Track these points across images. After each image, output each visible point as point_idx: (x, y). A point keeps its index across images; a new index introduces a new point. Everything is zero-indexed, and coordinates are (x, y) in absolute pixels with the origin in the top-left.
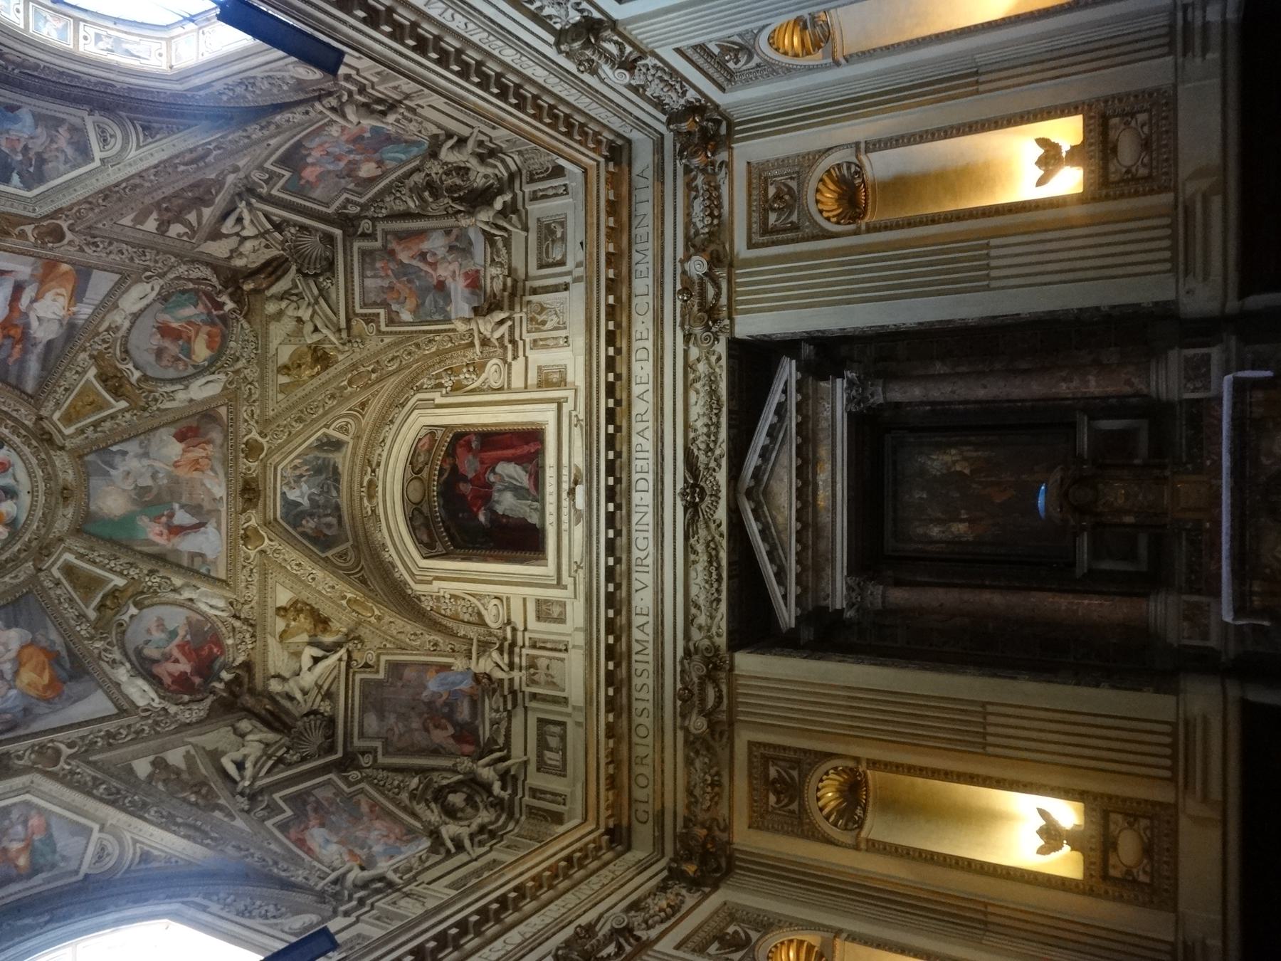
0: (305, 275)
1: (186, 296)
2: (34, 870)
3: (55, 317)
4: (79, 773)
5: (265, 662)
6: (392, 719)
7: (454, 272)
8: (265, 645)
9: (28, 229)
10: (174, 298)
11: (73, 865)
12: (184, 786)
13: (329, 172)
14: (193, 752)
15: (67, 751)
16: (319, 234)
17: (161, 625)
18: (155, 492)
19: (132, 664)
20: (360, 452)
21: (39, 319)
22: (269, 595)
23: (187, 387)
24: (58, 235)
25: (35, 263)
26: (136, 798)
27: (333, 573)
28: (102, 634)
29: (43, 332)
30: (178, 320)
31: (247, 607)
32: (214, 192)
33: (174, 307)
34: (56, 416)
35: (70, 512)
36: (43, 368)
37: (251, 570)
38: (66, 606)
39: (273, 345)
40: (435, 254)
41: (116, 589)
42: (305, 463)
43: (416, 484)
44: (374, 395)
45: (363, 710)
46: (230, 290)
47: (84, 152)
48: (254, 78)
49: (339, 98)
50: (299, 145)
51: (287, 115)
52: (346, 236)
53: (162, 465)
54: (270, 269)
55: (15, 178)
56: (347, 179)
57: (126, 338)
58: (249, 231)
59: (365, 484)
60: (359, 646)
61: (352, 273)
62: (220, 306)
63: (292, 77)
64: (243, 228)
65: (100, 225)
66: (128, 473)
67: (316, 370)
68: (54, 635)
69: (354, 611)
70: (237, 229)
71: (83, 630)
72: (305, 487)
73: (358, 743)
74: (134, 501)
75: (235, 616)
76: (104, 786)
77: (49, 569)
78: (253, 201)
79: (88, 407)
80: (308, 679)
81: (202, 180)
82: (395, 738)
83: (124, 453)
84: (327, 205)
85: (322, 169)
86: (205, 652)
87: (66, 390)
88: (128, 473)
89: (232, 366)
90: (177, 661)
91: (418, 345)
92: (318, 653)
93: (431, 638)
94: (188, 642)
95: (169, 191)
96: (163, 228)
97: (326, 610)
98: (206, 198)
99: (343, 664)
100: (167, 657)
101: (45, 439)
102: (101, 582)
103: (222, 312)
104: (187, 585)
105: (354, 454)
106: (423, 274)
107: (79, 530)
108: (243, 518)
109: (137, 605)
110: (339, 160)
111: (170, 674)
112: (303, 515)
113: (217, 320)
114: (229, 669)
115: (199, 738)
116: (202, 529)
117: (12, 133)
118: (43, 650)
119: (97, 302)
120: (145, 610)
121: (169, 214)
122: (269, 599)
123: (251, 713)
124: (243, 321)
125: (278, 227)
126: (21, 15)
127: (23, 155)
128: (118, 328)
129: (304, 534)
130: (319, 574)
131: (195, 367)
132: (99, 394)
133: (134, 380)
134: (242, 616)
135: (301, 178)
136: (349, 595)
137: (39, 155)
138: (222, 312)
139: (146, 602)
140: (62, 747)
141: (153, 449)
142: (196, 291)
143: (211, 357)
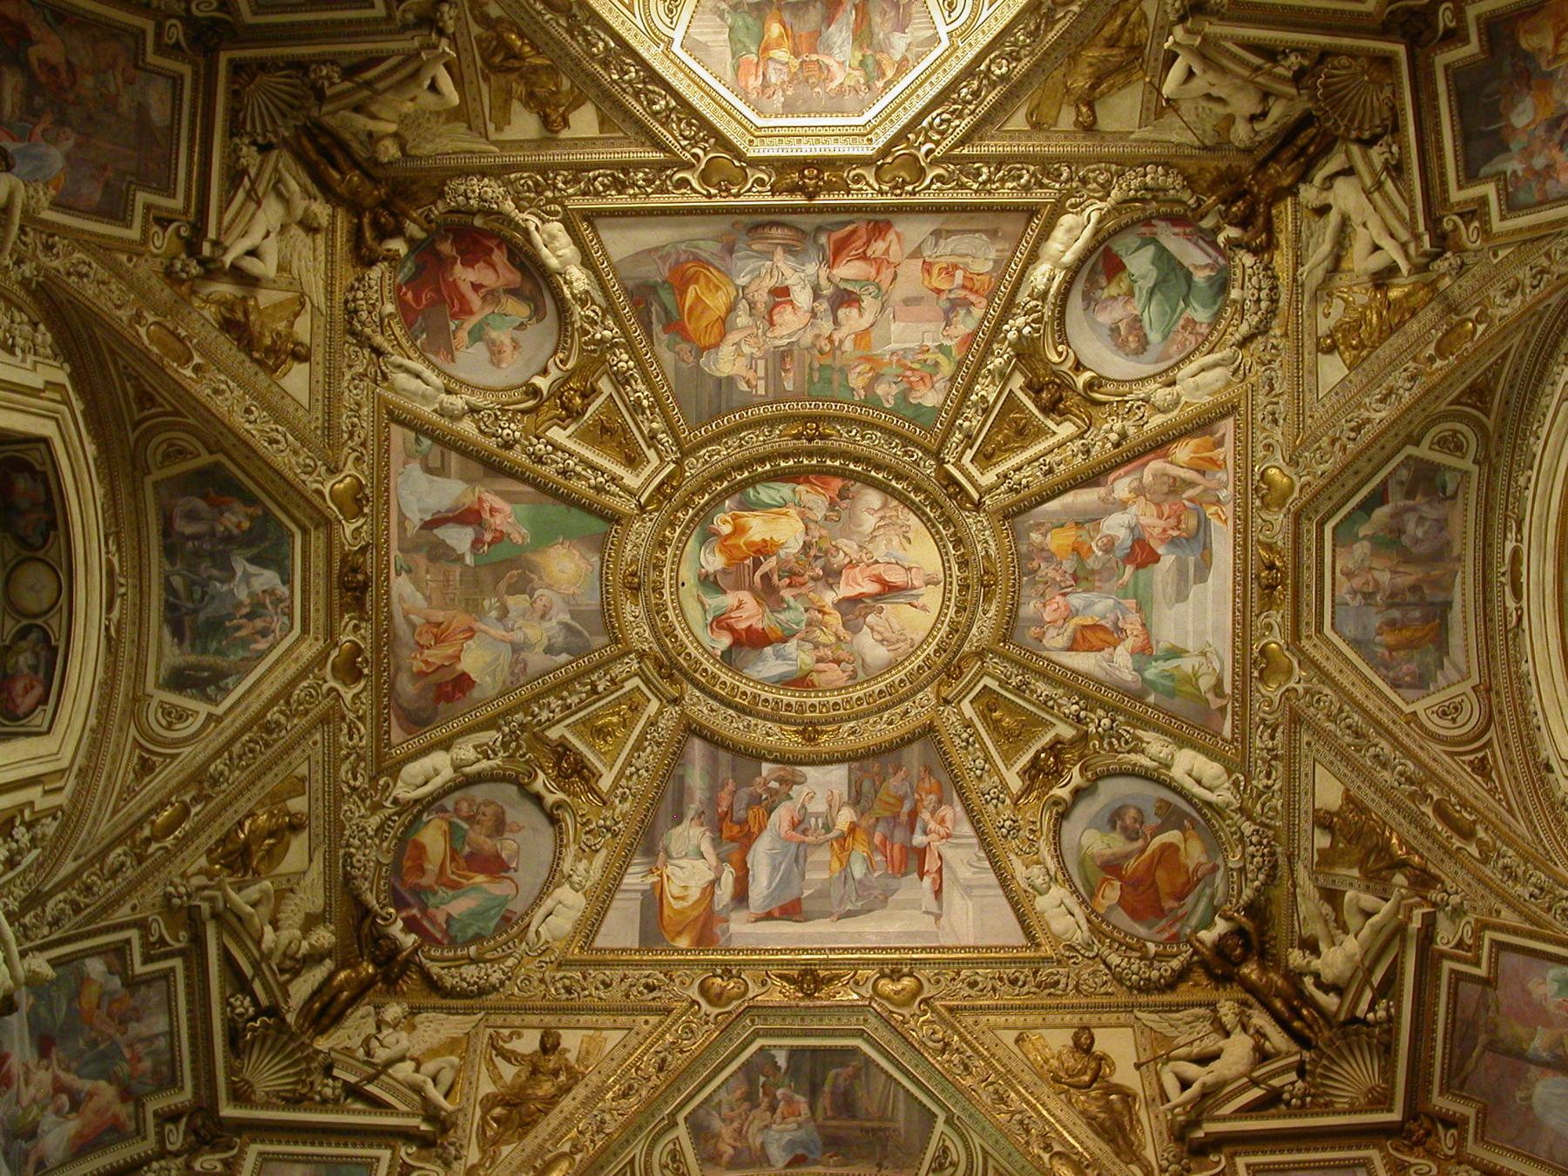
1: (470, 932)
3: (682, 862)
4: (685, 138)
5: (330, 262)
6: (125, 103)
7: (27, 1083)
8: (330, 293)
10: (492, 924)
16: (260, 1094)
17: (496, 353)
18: (503, 585)
20: (125, 670)
23: (457, 768)
28: (594, 351)
29: (690, 836)
30: (476, 888)
33: (488, 910)
34: (654, 705)
35: (628, 554)
36: (682, 778)
38: (645, 403)
40: (58, 1112)
41: (562, 422)
42: (245, 643)
43: (30, 602)
44: (128, 792)
45: (173, 130)
47: (699, 1130)
52: (204, 1108)
53: (492, 631)
55: (782, 1060)
57: (560, 845)
58: (405, 1070)
60: (178, 265)
62: (411, 925)
64: (417, 1070)
66: (543, 617)
68: (667, 357)
69: (181, 340)
70: (429, 1066)
71: (623, 360)
72: (242, 594)
74: (534, 568)
76: (657, 107)
78: (424, 1127)
80: (271, 213)
81: (521, 1138)
82: (122, 63)
83: (549, 650)
84: (264, 1158)
86: (426, 296)
88: (543, 617)
89: (389, 818)
90: (476, 287)
91: (77, 909)
92: (253, 266)
93: (56, 263)
94: (454, 316)
95: (567, 1104)
97: (226, 346)
99: (212, 234)
100: (491, 296)
102: (583, 436)
103: (404, 914)
104: (455, 418)
105: (140, 664)
106: (74, 1065)
107: (613, 518)
111: (492, 266)
113: (411, 901)
115: (475, 147)
116: (428, 518)
117: (794, 1126)
118: (687, 338)
119: (618, 896)
120: (519, 380)
121: (551, 1065)
123: (370, 169)
128: (578, 859)
129: (250, 500)
130: (238, 420)
131: (443, 810)
132: (592, 746)
133: (541, 776)
134: (367, 352)
137: (756, 1105)
138: (404, 914)
139: (518, 395)
140: (695, 185)
141: (506, 655)
142: (453, 943)
143: (417, 831)
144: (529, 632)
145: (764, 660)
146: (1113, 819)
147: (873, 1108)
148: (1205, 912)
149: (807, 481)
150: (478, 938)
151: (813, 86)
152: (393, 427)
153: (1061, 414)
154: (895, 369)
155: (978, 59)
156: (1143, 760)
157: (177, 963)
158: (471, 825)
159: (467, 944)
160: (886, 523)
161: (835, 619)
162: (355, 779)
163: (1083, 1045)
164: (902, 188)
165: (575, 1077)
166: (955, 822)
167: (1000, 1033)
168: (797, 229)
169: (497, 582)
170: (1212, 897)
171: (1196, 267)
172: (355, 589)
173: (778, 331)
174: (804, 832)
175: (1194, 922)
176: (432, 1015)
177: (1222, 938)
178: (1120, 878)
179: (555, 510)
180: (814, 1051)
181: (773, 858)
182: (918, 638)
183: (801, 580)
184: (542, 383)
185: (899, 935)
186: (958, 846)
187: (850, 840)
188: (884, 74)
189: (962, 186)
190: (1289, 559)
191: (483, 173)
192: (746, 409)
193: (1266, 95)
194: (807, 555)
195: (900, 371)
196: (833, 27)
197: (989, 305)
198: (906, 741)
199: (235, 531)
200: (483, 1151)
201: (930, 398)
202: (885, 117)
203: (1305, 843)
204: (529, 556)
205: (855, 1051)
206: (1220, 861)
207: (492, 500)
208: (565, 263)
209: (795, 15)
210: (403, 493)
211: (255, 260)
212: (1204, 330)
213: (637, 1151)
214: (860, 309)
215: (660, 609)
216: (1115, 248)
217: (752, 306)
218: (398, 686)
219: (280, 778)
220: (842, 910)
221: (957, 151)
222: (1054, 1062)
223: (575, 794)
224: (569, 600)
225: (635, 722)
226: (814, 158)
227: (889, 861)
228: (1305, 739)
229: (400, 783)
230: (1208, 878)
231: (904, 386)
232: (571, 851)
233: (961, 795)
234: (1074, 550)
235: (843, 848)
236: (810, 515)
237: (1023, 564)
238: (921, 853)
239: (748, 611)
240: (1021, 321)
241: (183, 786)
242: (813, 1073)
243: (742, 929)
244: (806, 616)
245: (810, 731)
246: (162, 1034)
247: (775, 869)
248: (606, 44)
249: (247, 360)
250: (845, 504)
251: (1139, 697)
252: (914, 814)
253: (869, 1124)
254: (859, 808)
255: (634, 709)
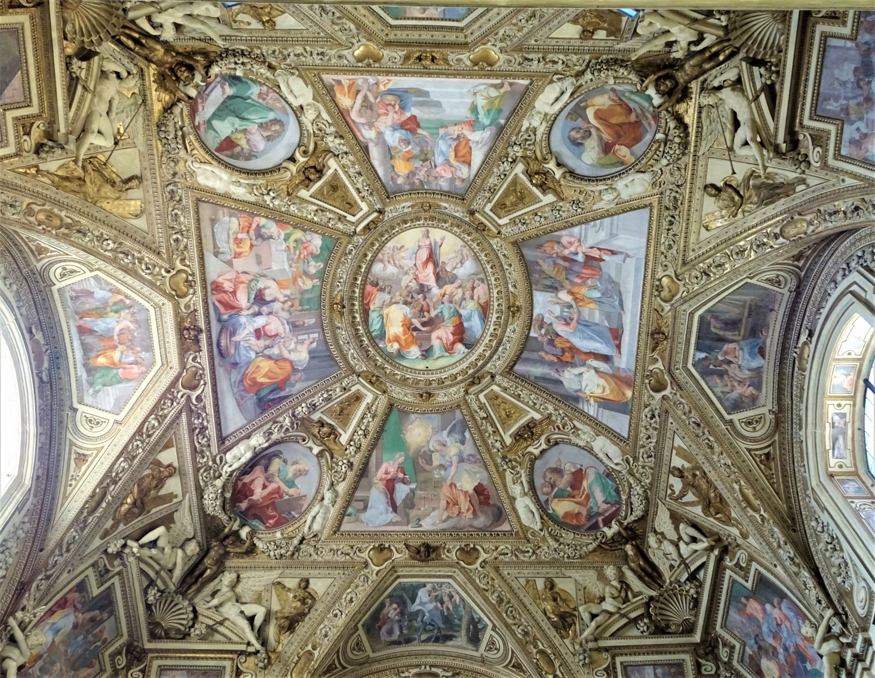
0: (647, 605)
1: (614, 493)
2: (90, 370)
3: (584, 385)
9: (660, 365)
10: (610, 483)
11: (88, 399)
12: (144, 493)
13: (760, 627)
14: (175, 501)
15: (194, 395)
16: (692, 619)
17: (301, 473)
18: (427, 467)
19: (267, 448)
20: (468, 664)
21: (582, 374)
22: (322, 571)
23: (525, 494)
24: (659, 387)
25: (629, 370)
26: (141, 450)
27: (340, 637)
28: (297, 424)
29: (569, 378)
30: (590, 487)
31: (312, 550)
32: (719, 516)
33: (602, 483)
34: (495, 388)
35: (410, 399)
36: (536, 378)
37: (348, 554)
38: (325, 396)
39: (572, 573)
41: (337, 436)
42: (456, 606)
46: (622, 531)
47: (736, 406)
48: (842, 550)
49: (843, 634)
50: (782, 596)
51: (811, 583)
52: (694, 649)
53: (452, 474)
54: (650, 570)
55: (703, 355)
56: (756, 647)
57: (570, 443)
58: (685, 550)
59: (434, 670)
60: (261, 665)
61: (657, 653)
62: (607, 522)
63: (852, 586)
64: (687, 544)
65: (671, 420)
66: (444, 445)
67: (552, 616)
68: (299, 386)
72: (431, 606)
73: (156, 663)
74: (418, 451)
75: (303, 539)
76: (156, 424)
77: (359, 383)
78: (716, 552)
79: (503, 413)
80: (231, 611)
84: (724, 626)
85: (761, 620)
86: (270, 512)
87: (519, 395)
88: (444, 445)
89: (549, 533)
90: (265, 487)
92: (258, 622)
94: (281, 497)
95: (712, 476)
96: (676, 473)
97: (302, 629)
98: (711, 510)
99: (243, 647)
100: (269, 479)
101: (475, 380)
102: (345, 424)
103: (601, 525)
105: (465, 657)
107: (391, 406)
108: (401, 546)
109: (320, 455)
110: (774, 638)
111: (252, 481)
112: (402, 604)
113: (594, 520)
114: (253, 533)
116: (391, 509)
117: (741, 352)
118: (288, 378)
119: (600, 419)
120: (315, 459)
121: (690, 477)
122: (317, 572)
123: (205, 552)
124: (595, 545)
125: (693, 577)
126: (846, 356)
127: (722, 361)
129: (382, 606)
130: (341, 621)
131: (547, 501)
132: (516, 421)
133: (531, 449)
134: (302, 547)
135: (747, 598)
136: (316, 653)
137: (726, 371)
138: (601, 525)
140: (198, 392)
141: (467, 466)
142: (619, 502)
143: (557, 516)
144: (452, 453)
145: (471, 327)
146: (577, 144)
147: (737, 311)
148: (641, 97)
149: (368, 304)
150: (617, 491)
151: (134, 337)
152: (343, 528)
153: (324, 166)
154: (301, 264)
155: (105, 259)
156: (542, 129)
157: (619, 660)
158: (556, 486)
159: (620, 498)
160: (392, 260)
161: (448, 288)
162: (528, 552)
163: (715, 190)
164: (190, 282)
165: (699, 468)
166: (571, 235)
167: (702, 238)
168: (221, 332)
169: (426, 471)
170: (631, 92)
171: (224, 93)
172: (429, 552)
173: (281, 330)
174: (572, 320)
175: (646, 104)
176: (656, 524)
177: (658, 91)
178: (614, 144)
179: (386, 438)
180: (699, 338)
181: (585, 338)
182: (460, 243)
183: (425, 306)
184: (316, 450)
185: (635, 281)
186: (586, 237)
187: (578, 296)
188: (122, 300)
189: (186, 247)
190: (415, 49)
191: (201, 497)
192: (326, 343)
193: (103, 74)
194: (410, 303)
195: (301, 261)
196: (96, 329)
197: (259, 215)
198: (522, 257)
199: (398, 610)
200: (733, 525)
201: (317, 242)
202: (148, 299)
203: (602, 43)
204: (411, 453)
205: (701, 318)
206: (609, 88)
207: (381, 473)
208: (249, 448)
209: (91, 350)
210: (377, 523)
211: (256, 618)
212: (265, 89)
213: (743, 446)
214: (265, 289)
215: (441, 382)
216: (217, 145)
217: (267, 347)
218: (481, 526)
219: (526, 594)
220: (618, 307)
221: (165, 256)
222: (724, 212)
223: (543, 431)
224: (436, 432)
225: (504, 398)
226: (177, 333)
227: (591, 276)
228: (533, 42)
229: (532, 526)
230: (619, 94)
231: (310, 258)
232: (574, 439)
233: (556, 231)
234: (408, 160)
235: (582, 300)
236: (387, 301)
237: (416, 190)
238: (588, 258)
239: (443, 334)
240: (267, 199)
241: (528, 654)
242: (712, 339)
243: (625, 361)
244: (446, 304)
245: (513, 310)
246: (655, 670)
247: (591, 338)
248: (124, 461)
249: (308, 616)
250: (381, 283)
251: (501, 129)
252: (565, 259)
253: (746, 314)
254: (559, 288)
255: (497, 397)
